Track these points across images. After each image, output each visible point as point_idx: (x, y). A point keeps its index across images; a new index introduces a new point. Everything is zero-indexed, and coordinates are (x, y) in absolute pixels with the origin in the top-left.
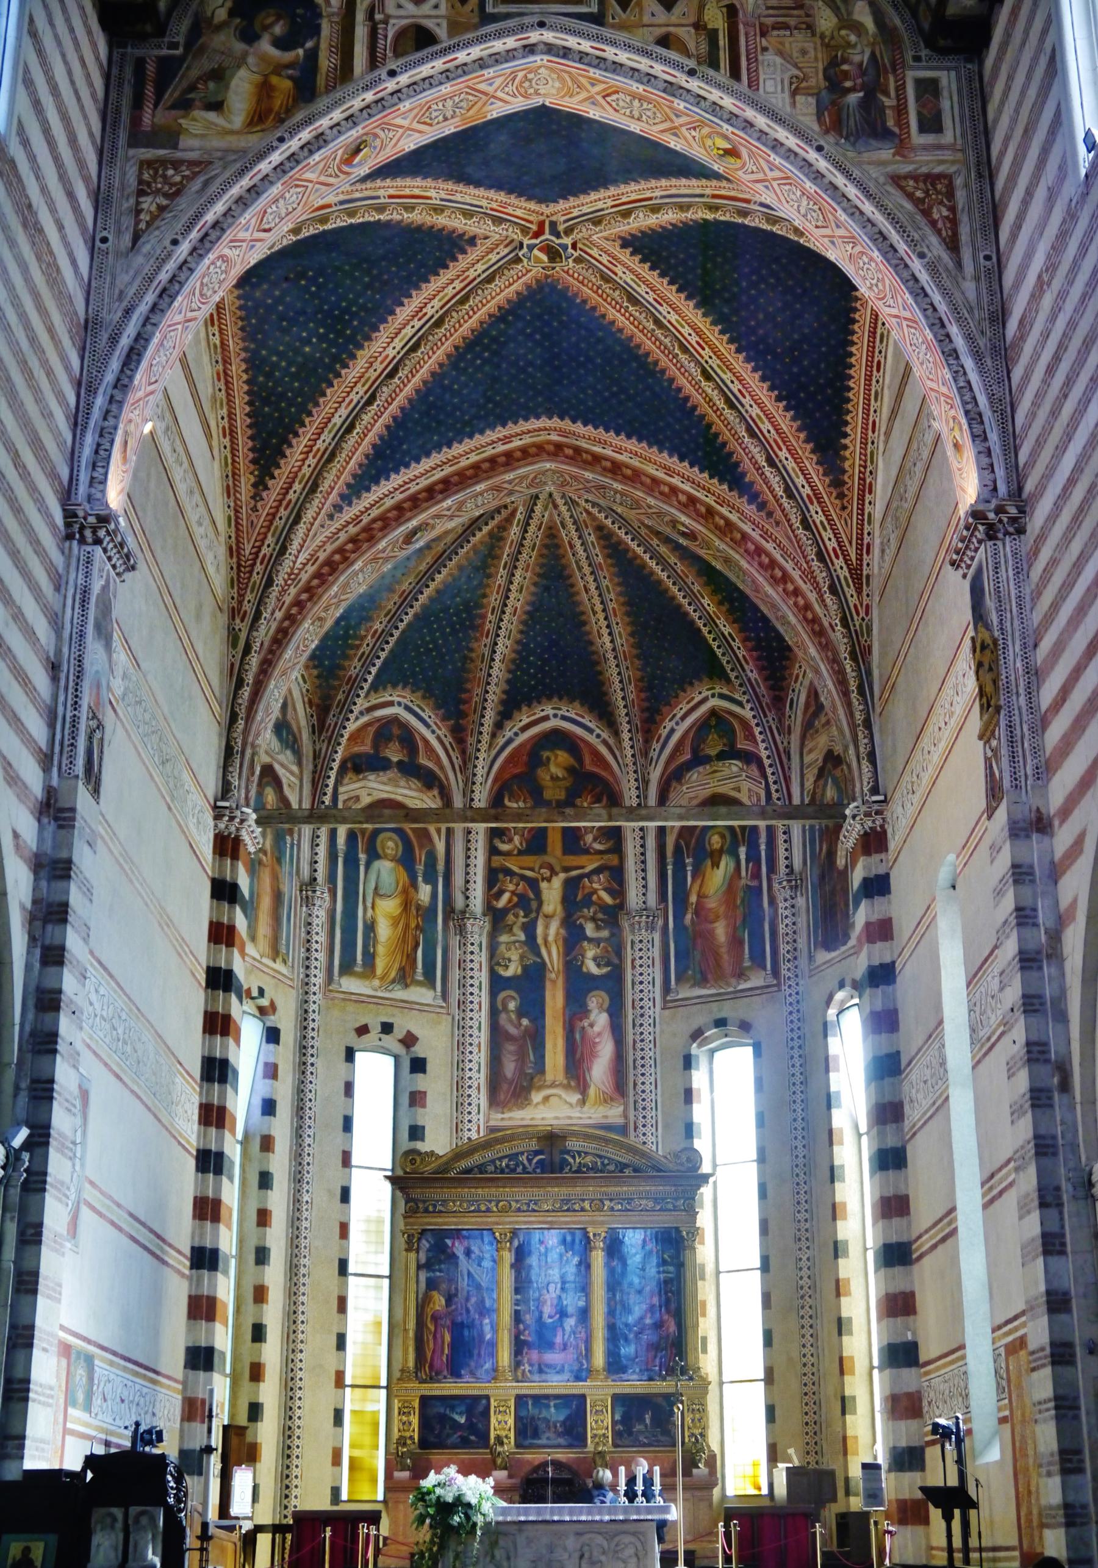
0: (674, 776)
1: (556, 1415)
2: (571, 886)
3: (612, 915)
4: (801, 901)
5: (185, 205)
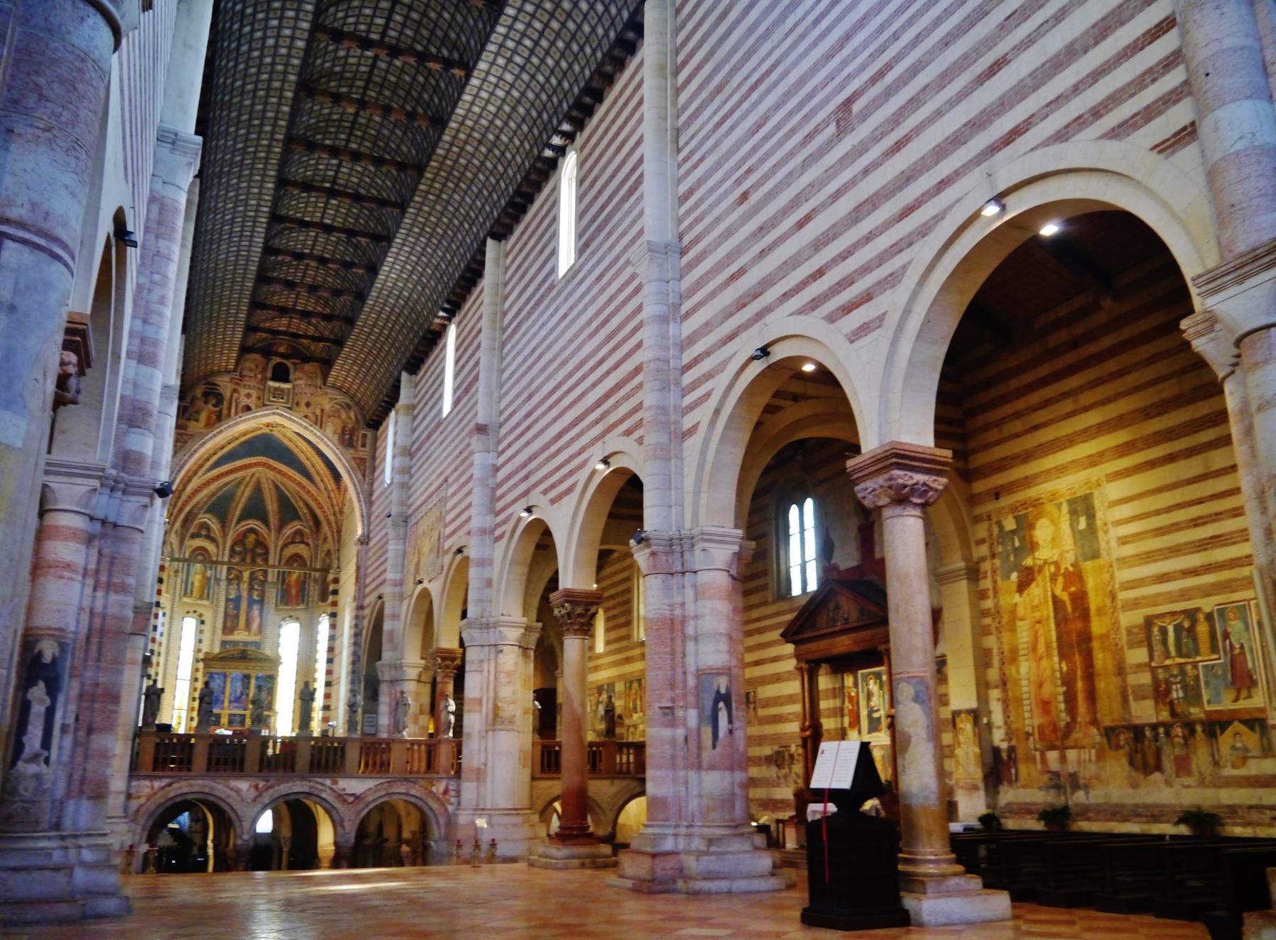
0: (286, 545)
1: (238, 719)
2: (252, 574)
3: (263, 583)
4: (317, 587)
5: (188, 446)
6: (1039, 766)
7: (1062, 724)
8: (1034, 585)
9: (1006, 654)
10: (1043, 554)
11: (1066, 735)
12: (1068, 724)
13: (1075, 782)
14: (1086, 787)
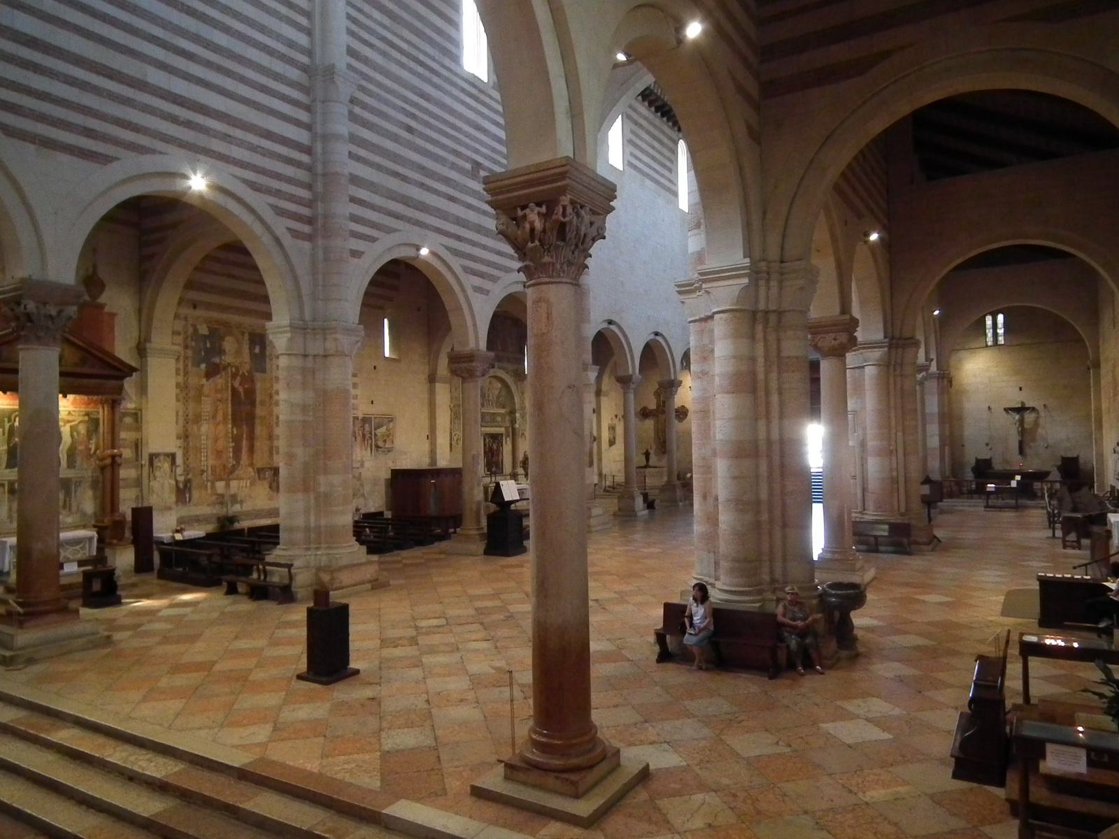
6: (209, 491)
7: (230, 465)
8: (219, 376)
9: (190, 416)
10: (228, 359)
11: (231, 472)
12: (233, 466)
13: (234, 499)
14: (241, 502)
